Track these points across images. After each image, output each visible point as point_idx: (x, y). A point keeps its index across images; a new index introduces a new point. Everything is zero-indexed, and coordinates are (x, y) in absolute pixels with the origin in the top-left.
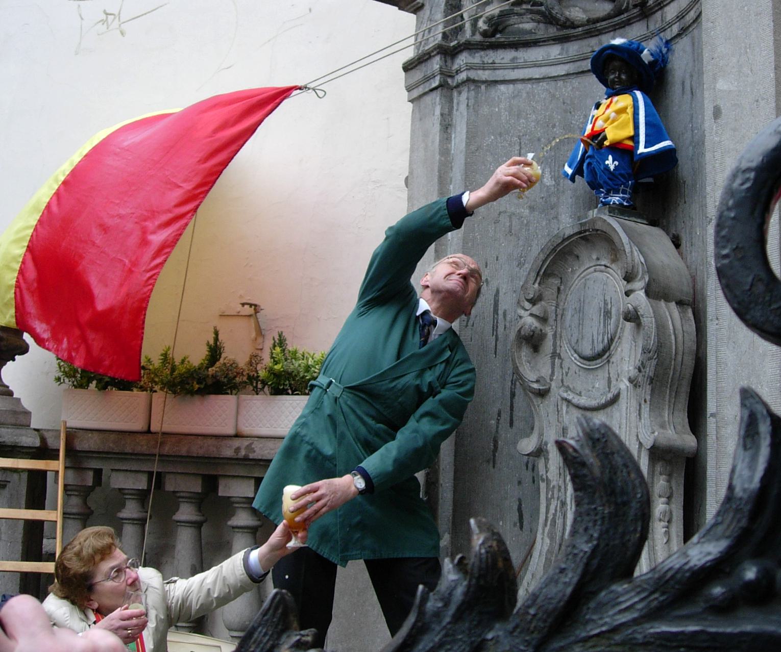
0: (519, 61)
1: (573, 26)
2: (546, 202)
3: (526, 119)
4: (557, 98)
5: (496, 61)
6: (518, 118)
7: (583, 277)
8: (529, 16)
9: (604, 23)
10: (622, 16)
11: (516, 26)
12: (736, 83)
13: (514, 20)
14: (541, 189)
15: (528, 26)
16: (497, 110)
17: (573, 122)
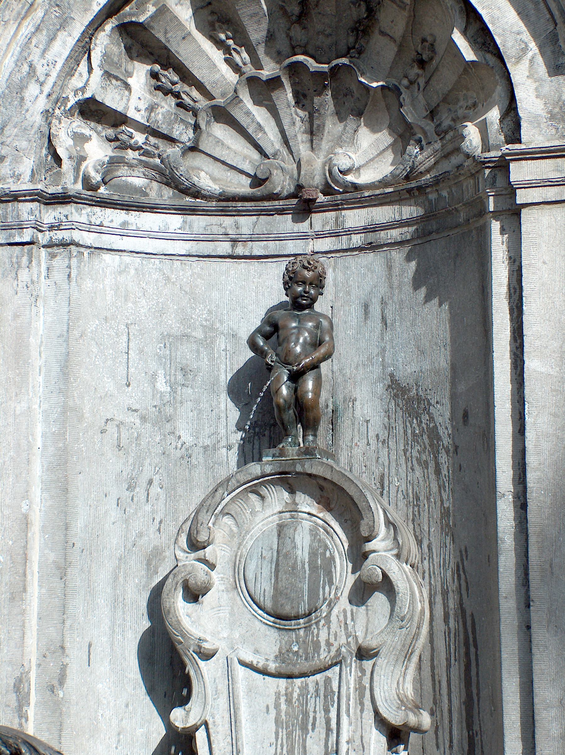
0: (130, 227)
1: (196, 193)
2: (160, 412)
3: (135, 303)
4: (173, 283)
5: (105, 224)
6: (126, 300)
8: (142, 170)
9: (246, 204)
10: (276, 203)
11: (124, 178)
12: (558, 369)
13: (123, 172)
14: (153, 395)
15: (139, 181)
16: (101, 286)
17: (194, 316)
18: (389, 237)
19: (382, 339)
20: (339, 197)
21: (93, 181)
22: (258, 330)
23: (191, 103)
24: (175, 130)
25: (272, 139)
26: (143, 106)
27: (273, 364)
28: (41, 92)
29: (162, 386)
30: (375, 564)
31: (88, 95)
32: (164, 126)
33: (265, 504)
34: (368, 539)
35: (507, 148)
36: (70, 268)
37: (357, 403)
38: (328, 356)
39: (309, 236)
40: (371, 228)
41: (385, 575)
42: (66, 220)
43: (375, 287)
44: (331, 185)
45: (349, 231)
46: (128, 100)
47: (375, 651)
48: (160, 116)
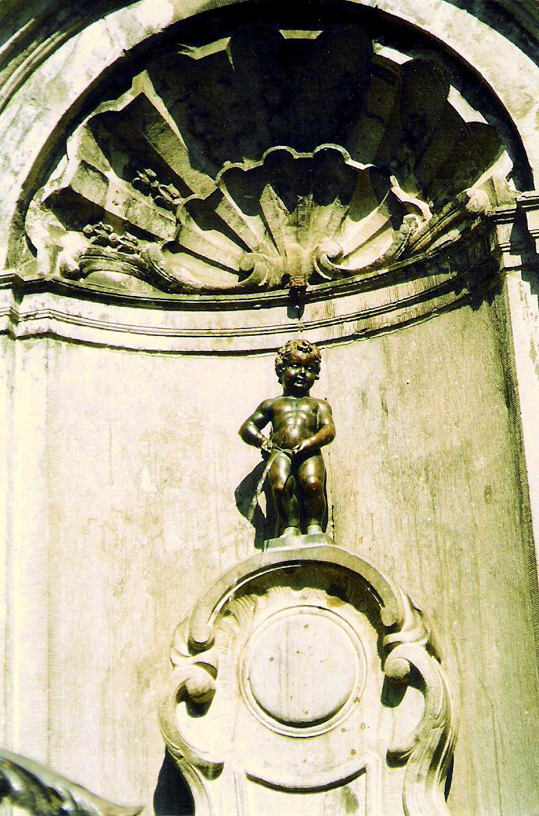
7: (279, 619)
11: (101, 272)
17: (178, 414)
18: (385, 321)
19: (384, 427)
20: (329, 284)
21: (71, 269)
22: (251, 418)
23: (170, 199)
24: (153, 226)
25: (255, 233)
26: (121, 199)
27: (270, 451)
28: (16, 182)
29: (147, 485)
30: (401, 656)
31: (65, 185)
32: (143, 223)
33: (270, 600)
34: (395, 628)
35: (520, 196)
36: (47, 358)
37: (359, 497)
38: (329, 439)
39: (297, 327)
40: (364, 314)
41: (413, 667)
42: (43, 308)
43: (372, 374)
44: (319, 274)
45: (341, 319)
46: (106, 193)
47: (405, 755)
48: (138, 211)
